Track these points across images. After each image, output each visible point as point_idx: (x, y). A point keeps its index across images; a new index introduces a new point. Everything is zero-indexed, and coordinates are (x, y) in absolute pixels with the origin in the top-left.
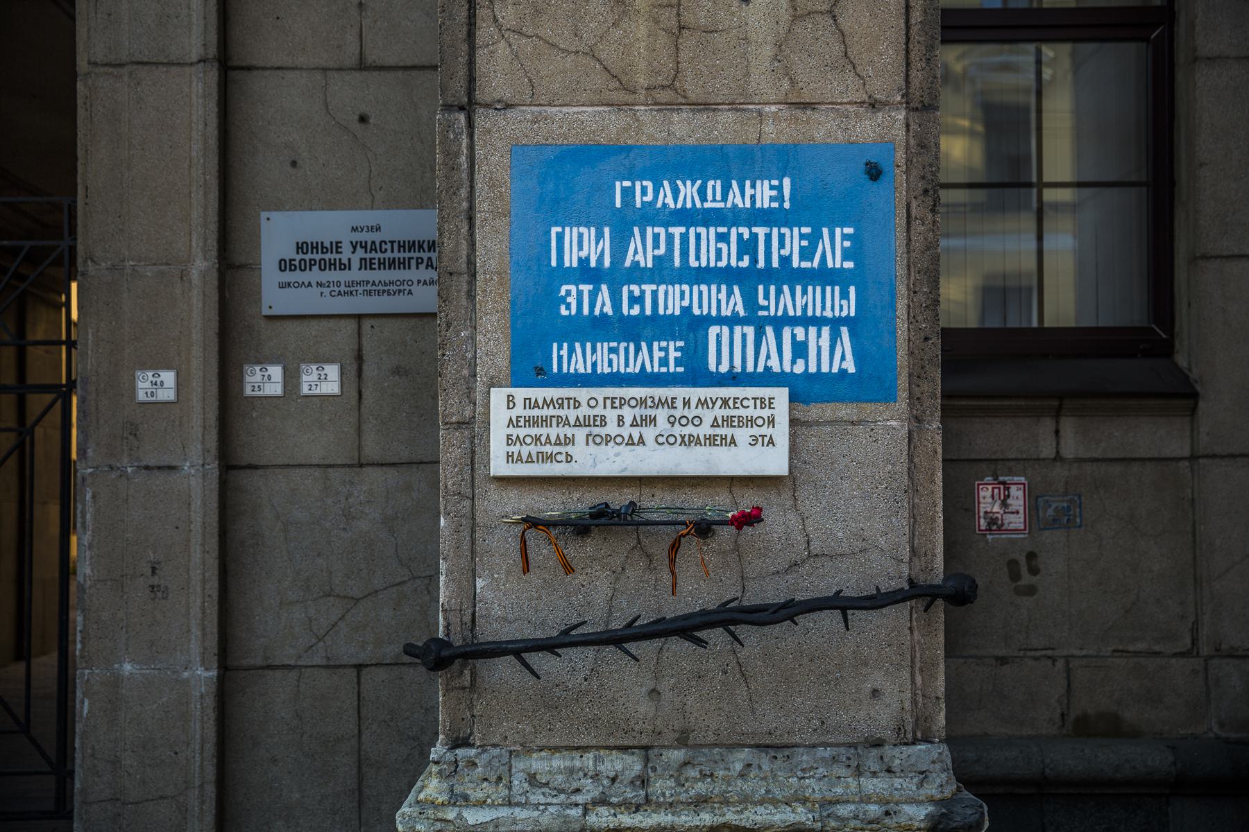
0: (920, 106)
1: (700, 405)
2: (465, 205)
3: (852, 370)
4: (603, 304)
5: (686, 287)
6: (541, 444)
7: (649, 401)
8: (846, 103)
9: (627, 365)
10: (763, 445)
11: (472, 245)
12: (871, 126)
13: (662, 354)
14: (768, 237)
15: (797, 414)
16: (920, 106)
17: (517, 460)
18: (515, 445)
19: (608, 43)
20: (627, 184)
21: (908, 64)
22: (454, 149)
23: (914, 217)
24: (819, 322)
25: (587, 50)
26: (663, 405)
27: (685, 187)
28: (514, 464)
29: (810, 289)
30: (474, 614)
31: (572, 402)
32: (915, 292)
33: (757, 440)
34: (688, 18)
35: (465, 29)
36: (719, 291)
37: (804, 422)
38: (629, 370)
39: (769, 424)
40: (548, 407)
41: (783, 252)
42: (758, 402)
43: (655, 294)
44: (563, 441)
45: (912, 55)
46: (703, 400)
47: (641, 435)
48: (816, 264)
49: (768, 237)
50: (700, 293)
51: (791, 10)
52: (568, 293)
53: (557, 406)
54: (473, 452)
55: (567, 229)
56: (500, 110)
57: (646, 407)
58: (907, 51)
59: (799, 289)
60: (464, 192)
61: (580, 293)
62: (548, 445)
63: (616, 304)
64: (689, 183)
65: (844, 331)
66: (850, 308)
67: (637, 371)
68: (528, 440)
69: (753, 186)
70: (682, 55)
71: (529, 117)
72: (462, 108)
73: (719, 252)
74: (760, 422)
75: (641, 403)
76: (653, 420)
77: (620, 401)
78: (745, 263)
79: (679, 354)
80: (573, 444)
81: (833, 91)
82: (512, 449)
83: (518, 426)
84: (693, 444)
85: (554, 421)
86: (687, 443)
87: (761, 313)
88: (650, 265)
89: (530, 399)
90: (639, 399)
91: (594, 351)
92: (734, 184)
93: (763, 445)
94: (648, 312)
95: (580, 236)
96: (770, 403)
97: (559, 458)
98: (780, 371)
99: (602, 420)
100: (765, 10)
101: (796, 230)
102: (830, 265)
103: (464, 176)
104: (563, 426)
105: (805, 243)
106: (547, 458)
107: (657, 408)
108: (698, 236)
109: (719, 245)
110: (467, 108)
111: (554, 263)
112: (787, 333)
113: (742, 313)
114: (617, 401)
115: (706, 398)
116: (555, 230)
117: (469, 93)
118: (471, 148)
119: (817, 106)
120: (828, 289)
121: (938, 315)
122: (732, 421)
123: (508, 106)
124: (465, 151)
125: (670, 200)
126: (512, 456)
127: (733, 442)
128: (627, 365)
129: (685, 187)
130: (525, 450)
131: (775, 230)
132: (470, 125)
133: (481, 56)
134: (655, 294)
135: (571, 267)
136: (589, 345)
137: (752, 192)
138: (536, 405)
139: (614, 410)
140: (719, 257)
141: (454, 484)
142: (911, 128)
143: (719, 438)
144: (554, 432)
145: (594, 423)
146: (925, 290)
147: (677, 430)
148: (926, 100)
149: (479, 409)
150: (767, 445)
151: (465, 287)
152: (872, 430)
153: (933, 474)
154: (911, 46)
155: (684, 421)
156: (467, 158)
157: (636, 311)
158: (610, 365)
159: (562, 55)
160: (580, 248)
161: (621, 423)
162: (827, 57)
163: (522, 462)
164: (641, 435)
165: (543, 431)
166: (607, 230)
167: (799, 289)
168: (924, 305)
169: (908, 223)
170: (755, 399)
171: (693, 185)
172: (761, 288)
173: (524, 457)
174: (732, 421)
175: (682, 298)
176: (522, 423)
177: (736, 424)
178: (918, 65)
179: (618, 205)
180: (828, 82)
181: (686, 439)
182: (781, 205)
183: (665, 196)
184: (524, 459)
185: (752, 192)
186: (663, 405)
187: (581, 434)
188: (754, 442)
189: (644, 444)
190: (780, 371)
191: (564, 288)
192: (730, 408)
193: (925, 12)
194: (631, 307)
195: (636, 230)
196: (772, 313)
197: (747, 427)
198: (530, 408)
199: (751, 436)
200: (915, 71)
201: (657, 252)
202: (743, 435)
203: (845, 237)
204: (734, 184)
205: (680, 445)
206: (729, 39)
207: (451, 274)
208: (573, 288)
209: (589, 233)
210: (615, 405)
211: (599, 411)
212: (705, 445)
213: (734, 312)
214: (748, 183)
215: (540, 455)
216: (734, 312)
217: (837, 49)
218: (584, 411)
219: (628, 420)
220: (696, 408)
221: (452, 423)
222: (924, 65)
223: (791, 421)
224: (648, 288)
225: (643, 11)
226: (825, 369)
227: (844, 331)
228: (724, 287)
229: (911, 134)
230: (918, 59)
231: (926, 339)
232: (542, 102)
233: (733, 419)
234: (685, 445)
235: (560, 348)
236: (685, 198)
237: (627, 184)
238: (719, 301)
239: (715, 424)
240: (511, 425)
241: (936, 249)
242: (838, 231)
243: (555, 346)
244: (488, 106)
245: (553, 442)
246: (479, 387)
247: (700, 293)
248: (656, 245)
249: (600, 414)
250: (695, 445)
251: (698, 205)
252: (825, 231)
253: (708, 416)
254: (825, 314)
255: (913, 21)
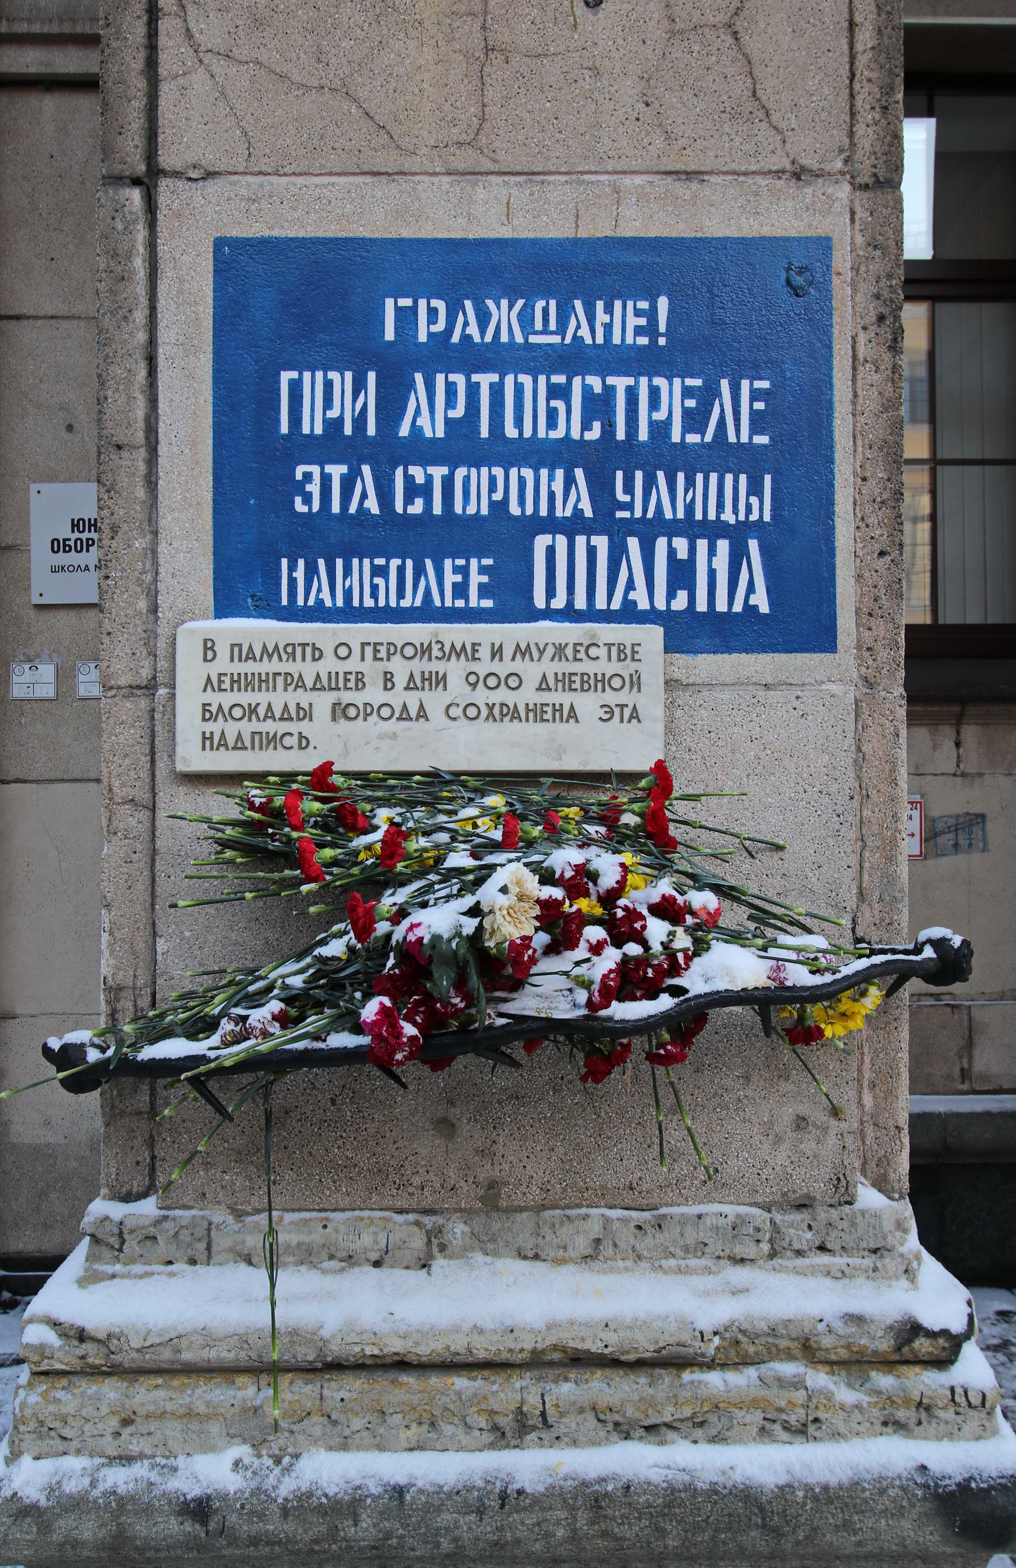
0: (870, 181)
1: (518, 656)
2: (142, 337)
3: (764, 608)
4: (364, 496)
5: (498, 472)
6: (259, 719)
7: (435, 648)
8: (754, 173)
9: (401, 594)
10: (622, 721)
11: (153, 401)
12: (796, 209)
13: (459, 578)
14: (632, 394)
15: (678, 674)
16: (870, 181)
17: (219, 745)
18: (215, 720)
19: (371, 74)
20: (406, 302)
21: (853, 115)
22: (122, 248)
23: (862, 359)
24: (714, 530)
25: (337, 83)
26: (458, 656)
27: (499, 308)
28: (214, 752)
29: (699, 477)
30: (154, 995)
31: (309, 650)
32: (864, 479)
33: (612, 713)
34: (501, 35)
35: (142, 55)
36: (551, 478)
37: (687, 685)
38: (406, 603)
39: (631, 687)
40: (270, 657)
41: (657, 416)
42: (614, 650)
43: (448, 483)
44: (294, 715)
45: (859, 102)
46: (523, 647)
47: (421, 705)
48: (708, 438)
49: (632, 394)
50: (522, 482)
51: (665, 22)
52: (308, 477)
53: (284, 657)
54: (153, 736)
55: (307, 375)
56: (196, 180)
57: (430, 659)
58: (852, 96)
59: (681, 477)
60: (140, 316)
61: (326, 480)
62: (270, 721)
63: (385, 497)
64: (504, 303)
65: (753, 545)
66: (762, 509)
67: (418, 603)
68: (237, 713)
69: (609, 309)
70: (490, 93)
71: (243, 191)
72: (136, 182)
73: (552, 416)
74: (616, 683)
75: (423, 653)
76: (440, 681)
77: (388, 650)
78: (594, 433)
79: (485, 579)
80: (311, 720)
81: (733, 152)
82: (210, 727)
83: (220, 690)
84: (507, 719)
85: (280, 680)
86: (498, 717)
87: (620, 514)
88: (440, 433)
89: (240, 646)
90: (418, 646)
91: (347, 572)
92: (578, 304)
93: (622, 721)
94: (437, 509)
95: (328, 385)
96: (634, 652)
97: (288, 741)
98: (648, 607)
99: (357, 680)
100: (624, 22)
101: (677, 382)
102: (732, 438)
103: (141, 290)
104: (295, 690)
105: (691, 403)
106: (269, 743)
107: (449, 659)
108: (519, 389)
109: (553, 403)
110: (146, 180)
111: (284, 429)
112: (661, 543)
113: (589, 513)
114: (383, 650)
115: (528, 645)
116: (286, 377)
117: (148, 158)
118: (152, 245)
119: (706, 178)
120: (729, 478)
121: (900, 516)
122: (571, 682)
123: (210, 175)
124: (141, 250)
125: (473, 330)
126: (211, 738)
127: (573, 714)
128: (401, 594)
129: (499, 308)
130: (232, 730)
131: (644, 381)
132: (151, 207)
133: (167, 92)
134: (448, 483)
135: (311, 436)
136: (339, 563)
137: (607, 319)
138: (251, 656)
139: (378, 663)
140: (552, 423)
141: (123, 785)
142: (857, 217)
143: (549, 709)
144: (279, 698)
145: (345, 685)
146: (880, 475)
147: (482, 696)
148: (882, 174)
149: (162, 664)
150: (629, 721)
151: (142, 468)
152: (798, 698)
153: (893, 770)
154: (857, 87)
155: (492, 682)
156: (144, 261)
157: (417, 507)
158: (374, 595)
159: (296, 93)
160: (328, 404)
161: (389, 685)
162: (724, 98)
163: (227, 749)
164: (421, 705)
165: (261, 698)
166: (372, 377)
167: (681, 477)
168: (879, 499)
169: (854, 369)
170: (610, 645)
171: (511, 307)
172: (619, 475)
173: (231, 741)
174: (571, 682)
175: (492, 488)
176: (227, 685)
177: (577, 685)
178: (867, 116)
179: (390, 335)
180: (725, 138)
181: (496, 711)
182: (654, 342)
183: (466, 324)
184: (231, 743)
185: (607, 319)
186: (458, 656)
187: (323, 702)
188: (608, 716)
189: (427, 720)
190: (648, 607)
191: (300, 471)
192: (567, 660)
193: (879, 32)
194: (408, 500)
195: (419, 377)
196: (638, 514)
197: (596, 690)
198: (240, 660)
199: (602, 706)
200: (864, 126)
201: (452, 414)
202: (588, 704)
203: (755, 395)
204: (578, 304)
205: (487, 719)
206: (565, 69)
207: (119, 447)
208: (315, 470)
209: (343, 381)
210: (379, 656)
211: (353, 665)
212: (527, 720)
213: (578, 512)
214: (600, 305)
215: (257, 738)
216: (578, 512)
217: (740, 86)
218: (328, 665)
219: (401, 680)
220: (513, 659)
221: (119, 688)
222: (877, 117)
223: (666, 683)
224: (438, 472)
225: (426, 22)
226: (721, 606)
227: (753, 545)
228: (560, 473)
229: (857, 227)
230: (868, 107)
231: (882, 554)
232: (264, 169)
233: (573, 678)
234: (495, 720)
235: (292, 568)
236: (498, 327)
237: (406, 302)
238: (552, 495)
239: (543, 686)
240: (209, 688)
241: (898, 409)
242: (745, 384)
243: (284, 562)
244: (177, 174)
245: (278, 715)
246: (163, 630)
247: (522, 482)
248: (450, 402)
249: (354, 670)
250: (511, 721)
251: (519, 339)
252: (725, 384)
253: (531, 671)
254: (723, 517)
255: (859, 47)
